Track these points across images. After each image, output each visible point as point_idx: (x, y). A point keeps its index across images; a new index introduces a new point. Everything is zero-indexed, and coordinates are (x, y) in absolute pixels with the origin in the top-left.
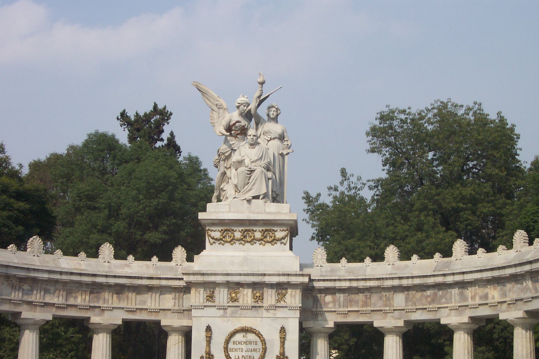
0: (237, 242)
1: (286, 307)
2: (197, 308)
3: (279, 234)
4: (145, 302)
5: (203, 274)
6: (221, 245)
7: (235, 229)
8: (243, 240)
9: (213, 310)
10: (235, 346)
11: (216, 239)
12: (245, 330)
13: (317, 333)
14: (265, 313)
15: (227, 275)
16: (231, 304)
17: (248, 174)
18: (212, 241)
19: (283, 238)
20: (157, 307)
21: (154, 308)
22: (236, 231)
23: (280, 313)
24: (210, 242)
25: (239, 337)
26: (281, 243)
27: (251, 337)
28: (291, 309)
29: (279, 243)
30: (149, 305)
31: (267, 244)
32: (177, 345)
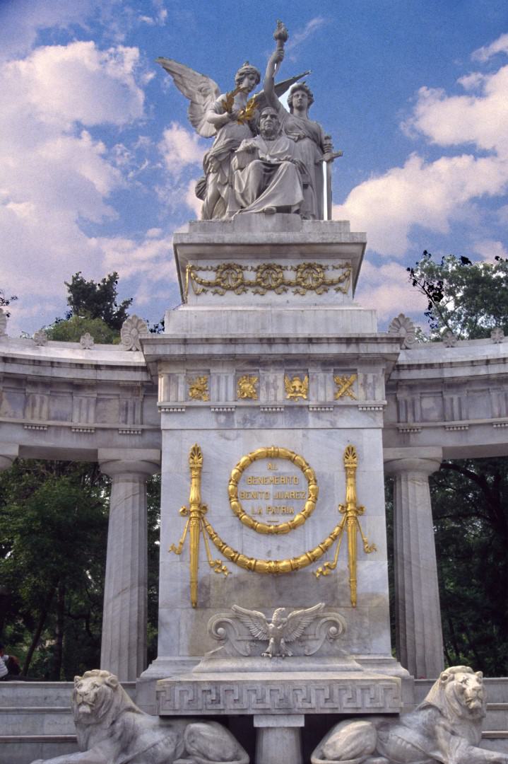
0: (250, 290)
1: (357, 406)
2: (170, 411)
3: (332, 275)
4: (69, 417)
5: (185, 342)
6: (217, 295)
7: (244, 263)
8: (260, 287)
9: (206, 419)
10: (253, 489)
11: (209, 285)
12: (272, 456)
13: (406, 470)
14: (312, 421)
15: (232, 341)
16: (241, 403)
17: (265, 170)
18: (200, 288)
19: (340, 281)
20: (92, 423)
21: (85, 425)
22: (246, 268)
23: (344, 421)
24: (195, 291)
25: (261, 469)
26: (338, 290)
27: (284, 468)
28: (367, 410)
29: (332, 291)
30: (76, 420)
31: (309, 292)
32: (130, 499)
